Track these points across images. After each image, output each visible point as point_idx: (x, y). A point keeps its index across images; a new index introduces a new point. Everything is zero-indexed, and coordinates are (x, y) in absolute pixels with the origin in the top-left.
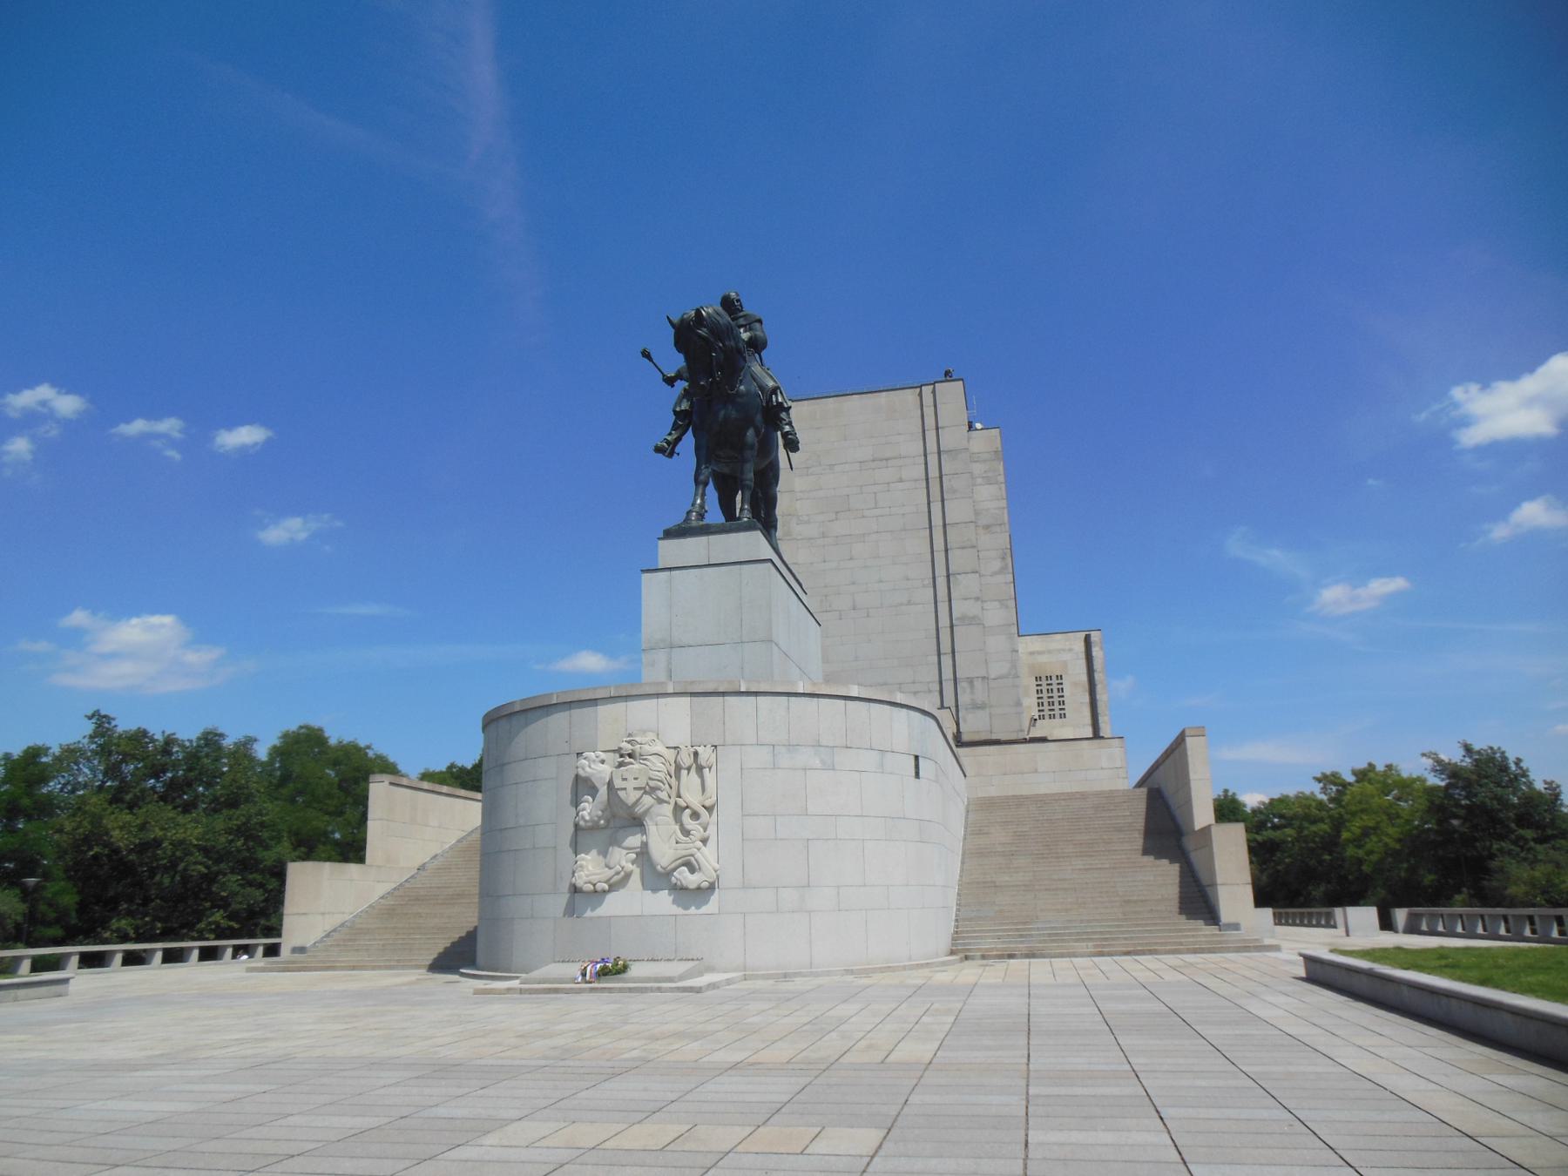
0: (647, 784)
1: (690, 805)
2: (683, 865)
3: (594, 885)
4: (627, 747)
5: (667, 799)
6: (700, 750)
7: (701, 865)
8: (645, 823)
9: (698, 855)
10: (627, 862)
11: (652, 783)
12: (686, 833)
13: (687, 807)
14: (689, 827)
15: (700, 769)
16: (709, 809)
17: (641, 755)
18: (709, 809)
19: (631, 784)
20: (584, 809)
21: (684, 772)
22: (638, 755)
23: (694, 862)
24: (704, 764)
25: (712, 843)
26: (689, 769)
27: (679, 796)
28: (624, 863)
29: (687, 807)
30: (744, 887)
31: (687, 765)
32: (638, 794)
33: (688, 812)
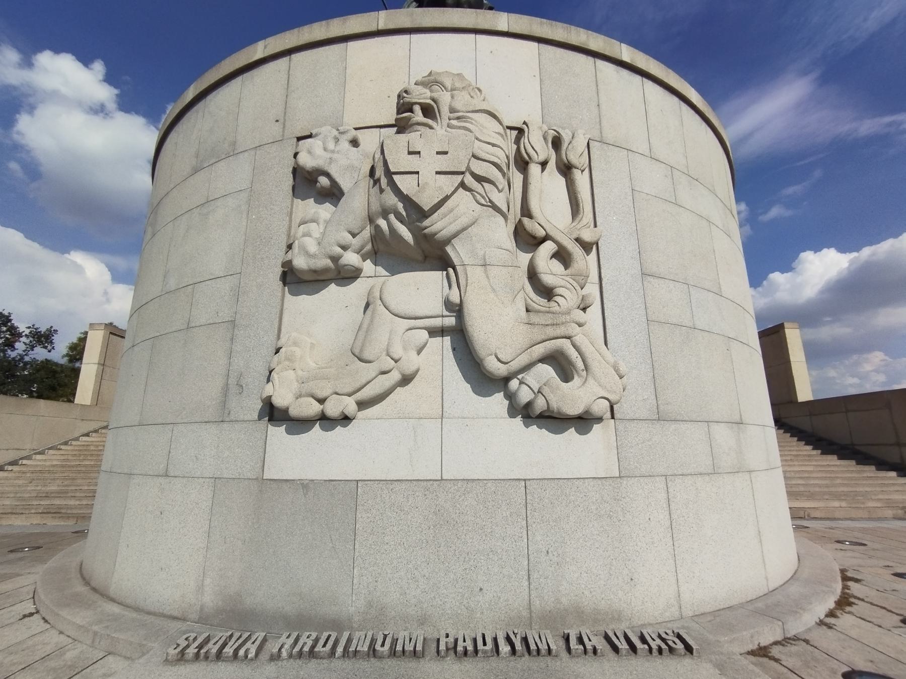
0: (468, 169)
1: (552, 233)
2: (543, 360)
3: (321, 401)
4: (422, 95)
5: (505, 209)
6: (566, 136)
7: (590, 361)
8: (456, 261)
9: (578, 339)
10: (405, 349)
11: (480, 168)
12: (547, 293)
13: (547, 238)
14: (548, 279)
15: (566, 169)
16: (587, 247)
17: (452, 110)
18: (587, 247)
19: (428, 164)
20: (307, 234)
21: (535, 169)
22: (445, 110)
23: (573, 354)
24: (573, 158)
25: (595, 311)
26: (544, 164)
27: (526, 211)
28: (397, 352)
29: (547, 238)
30: (660, 417)
31: (542, 158)
32: (448, 184)
33: (548, 248)
